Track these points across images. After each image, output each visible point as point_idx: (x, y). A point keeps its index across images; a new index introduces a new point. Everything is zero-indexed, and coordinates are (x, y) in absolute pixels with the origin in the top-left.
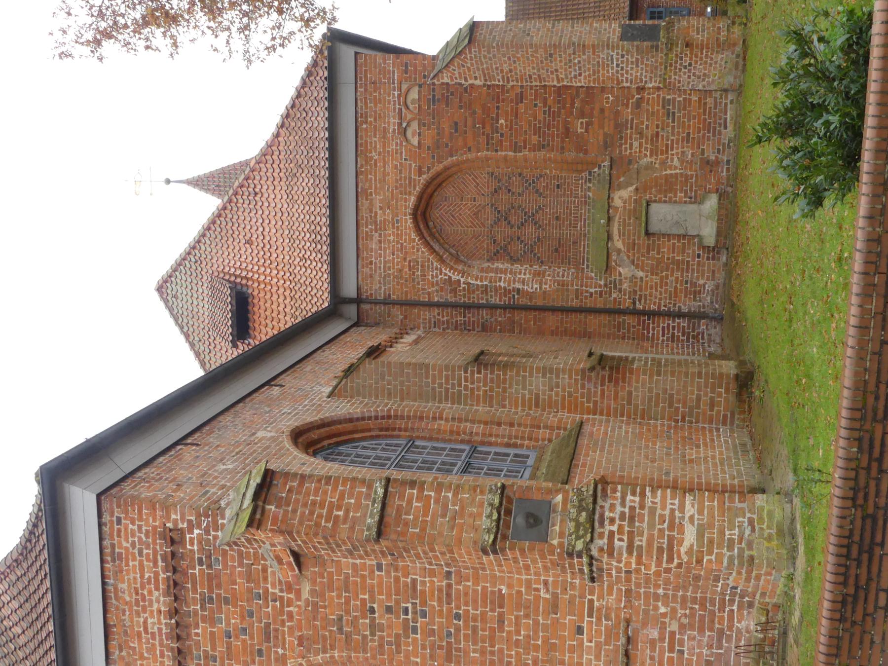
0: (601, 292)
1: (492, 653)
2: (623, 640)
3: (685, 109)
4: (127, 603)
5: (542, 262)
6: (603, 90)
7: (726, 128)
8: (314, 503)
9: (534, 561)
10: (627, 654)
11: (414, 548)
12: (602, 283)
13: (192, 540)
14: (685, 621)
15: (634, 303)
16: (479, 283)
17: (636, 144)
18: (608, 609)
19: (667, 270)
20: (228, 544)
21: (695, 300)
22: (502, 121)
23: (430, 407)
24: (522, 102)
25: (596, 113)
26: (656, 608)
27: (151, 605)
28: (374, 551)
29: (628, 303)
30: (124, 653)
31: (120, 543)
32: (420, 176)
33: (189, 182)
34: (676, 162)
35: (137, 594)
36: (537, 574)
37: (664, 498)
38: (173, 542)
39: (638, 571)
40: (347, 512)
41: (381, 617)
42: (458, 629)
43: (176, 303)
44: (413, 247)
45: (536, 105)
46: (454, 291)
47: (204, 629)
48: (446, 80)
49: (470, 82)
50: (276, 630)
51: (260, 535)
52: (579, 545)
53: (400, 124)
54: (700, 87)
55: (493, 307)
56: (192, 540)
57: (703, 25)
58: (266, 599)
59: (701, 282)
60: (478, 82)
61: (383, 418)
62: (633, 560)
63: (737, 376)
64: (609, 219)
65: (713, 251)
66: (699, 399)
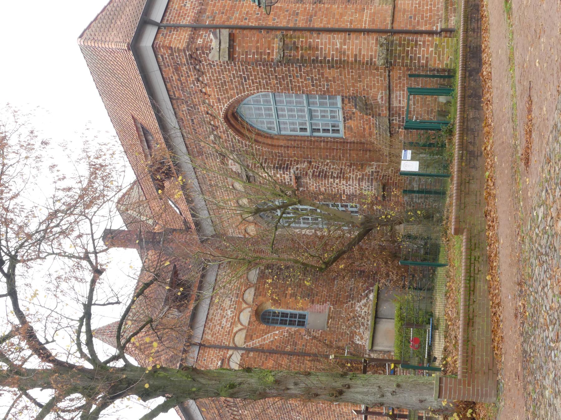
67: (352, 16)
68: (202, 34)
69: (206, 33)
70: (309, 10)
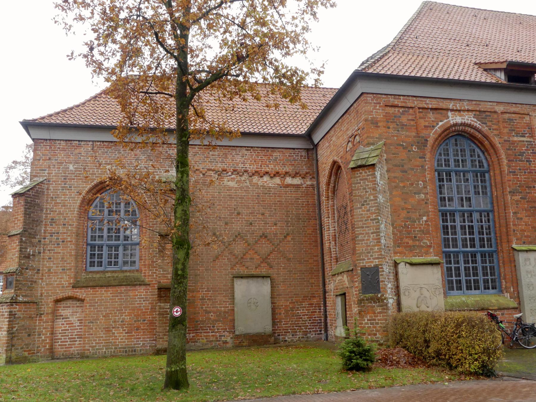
57: (377, 323)
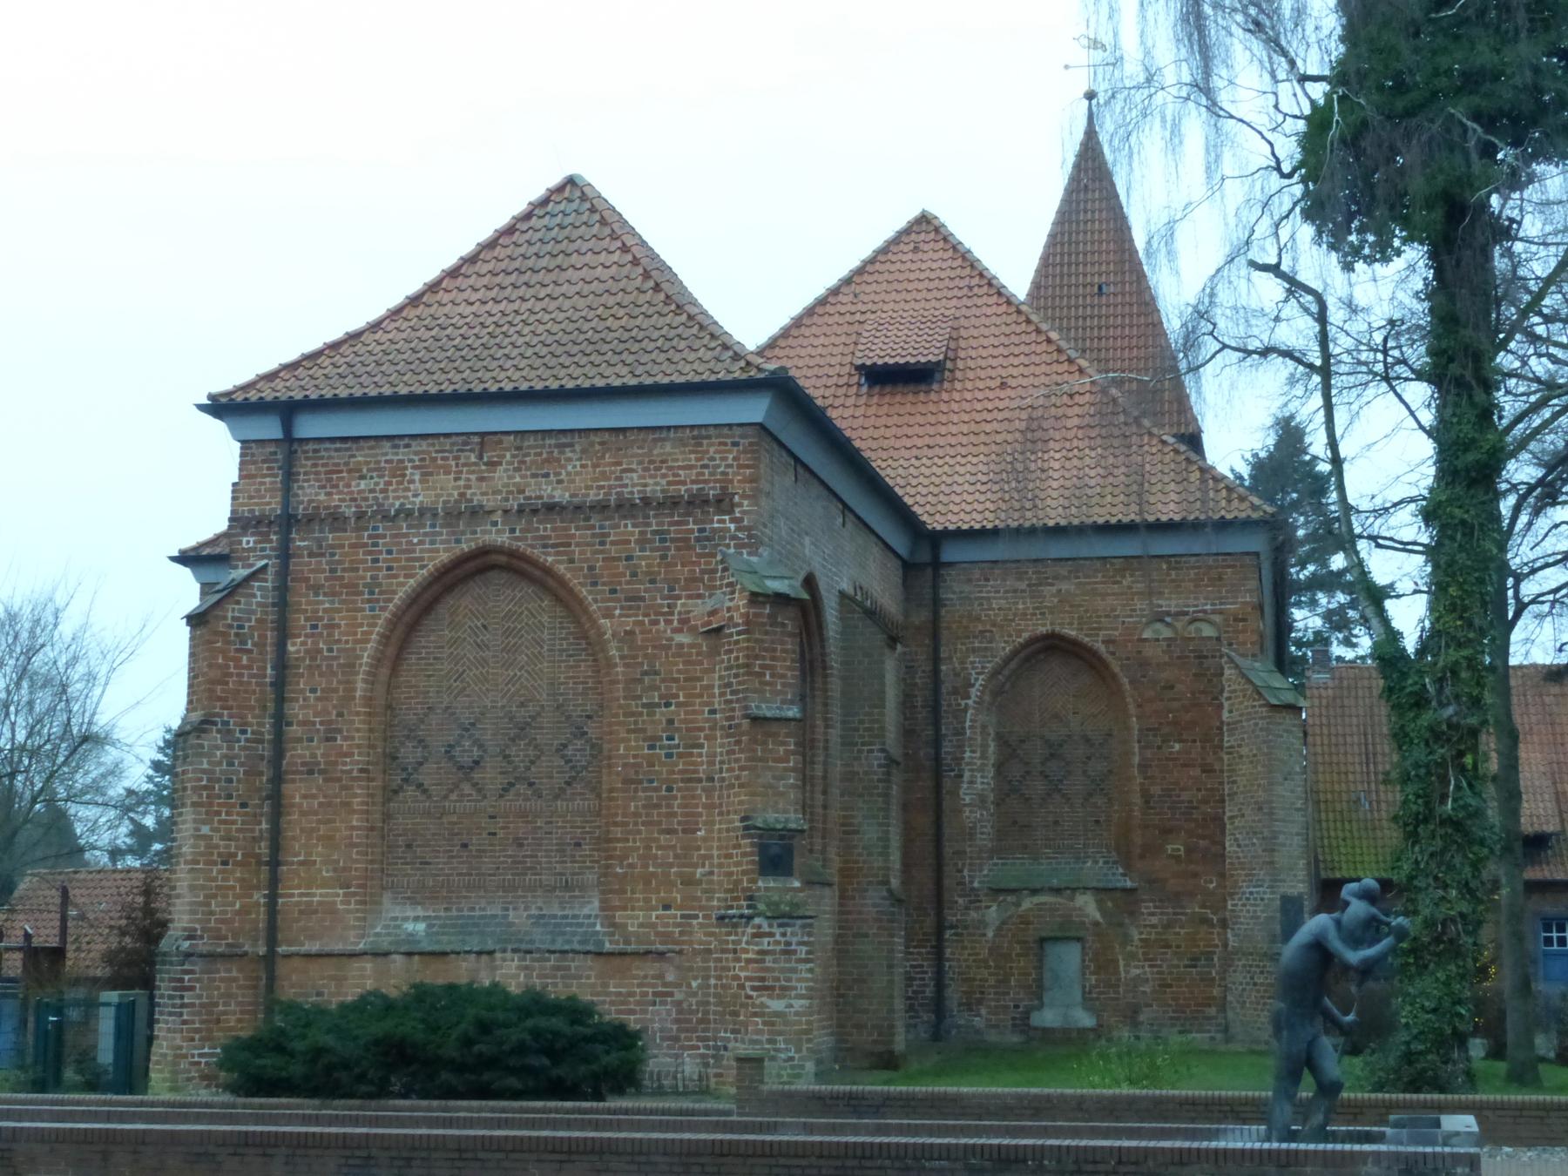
0: (963, 884)
1: (636, 824)
2: (661, 948)
3: (1202, 980)
4: (651, 450)
5: (998, 805)
6: (1222, 875)
7: (1180, 1032)
8: (775, 650)
9: (738, 864)
10: (648, 953)
11: (741, 751)
12: (976, 885)
13: (723, 521)
14: (685, 1006)
15: (952, 927)
16: (968, 724)
17: (1154, 920)
18: (691, 933)
19: (996, 967)
20: (722, 562)
21: (960, 1005)
22: (1177, 747)
23: (836, 712)
24: (1204, 771)
25: (1192, 867)
26: (695, 978)
27: (651, 477)
28: (733, 710)
29: (951, 919)
30: (597, 447)
31: (712, 445)
32: (1106, 642)
33: (1091, 135)
34: (1135, 972)
35: (663, 462)
36: (720, 865)
37: (807, 980)
38: (719, 501)
39: (738, 960)
40: (767, 683)
41: (662, 714)
42: (657, 789)
43: (906, 248)
44: (1010, 636)
45: (1199, 790)
46: (955, 692)
47: (632, 534)
48: (1227, 672)
49: (1226, 704)
50: (639, 608)
51: (741, 602)
52: (761, 907)
53: (1168, 614)
54: (1229, 998)
55: (937, 741)
56: (723, 521)
58: (669, 597)
59: (983, 1011)
60: (1225, 715)
61: (824, 661)
62: (750, 956)
63: (891, 1053)
64: (1057, 891)
65: (1023, 1024)
66: (866, 1011)
67: (324, 863)
68: (271, 541)
69: (272, 549)
70: (345, 764)
